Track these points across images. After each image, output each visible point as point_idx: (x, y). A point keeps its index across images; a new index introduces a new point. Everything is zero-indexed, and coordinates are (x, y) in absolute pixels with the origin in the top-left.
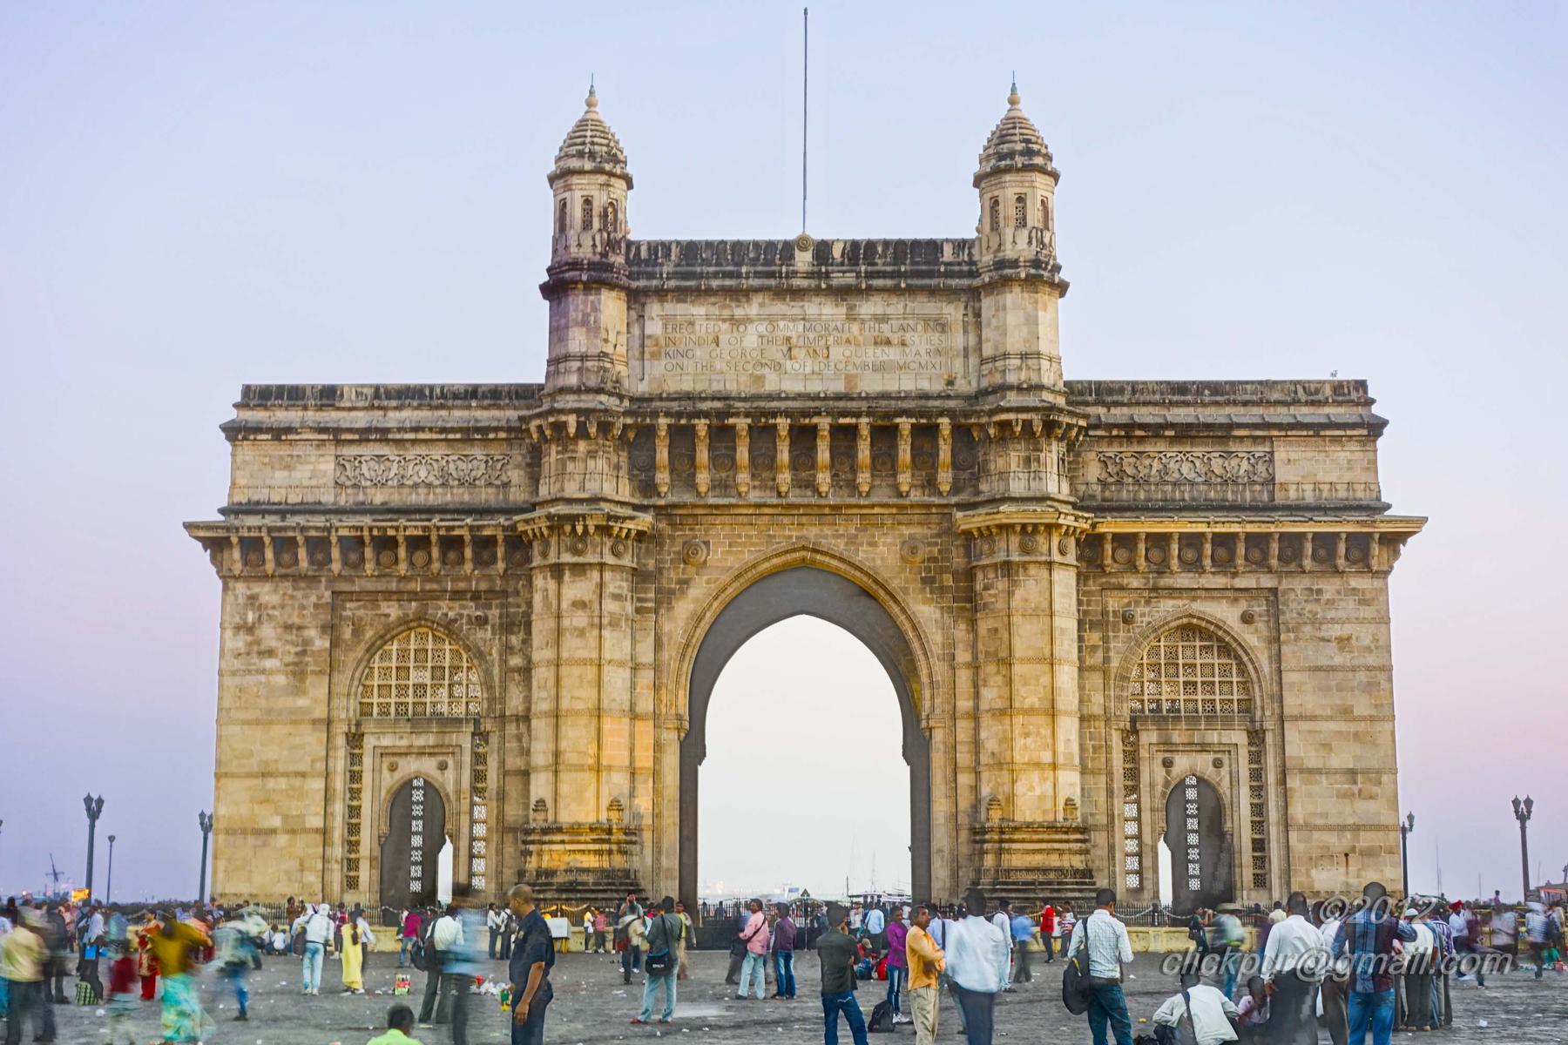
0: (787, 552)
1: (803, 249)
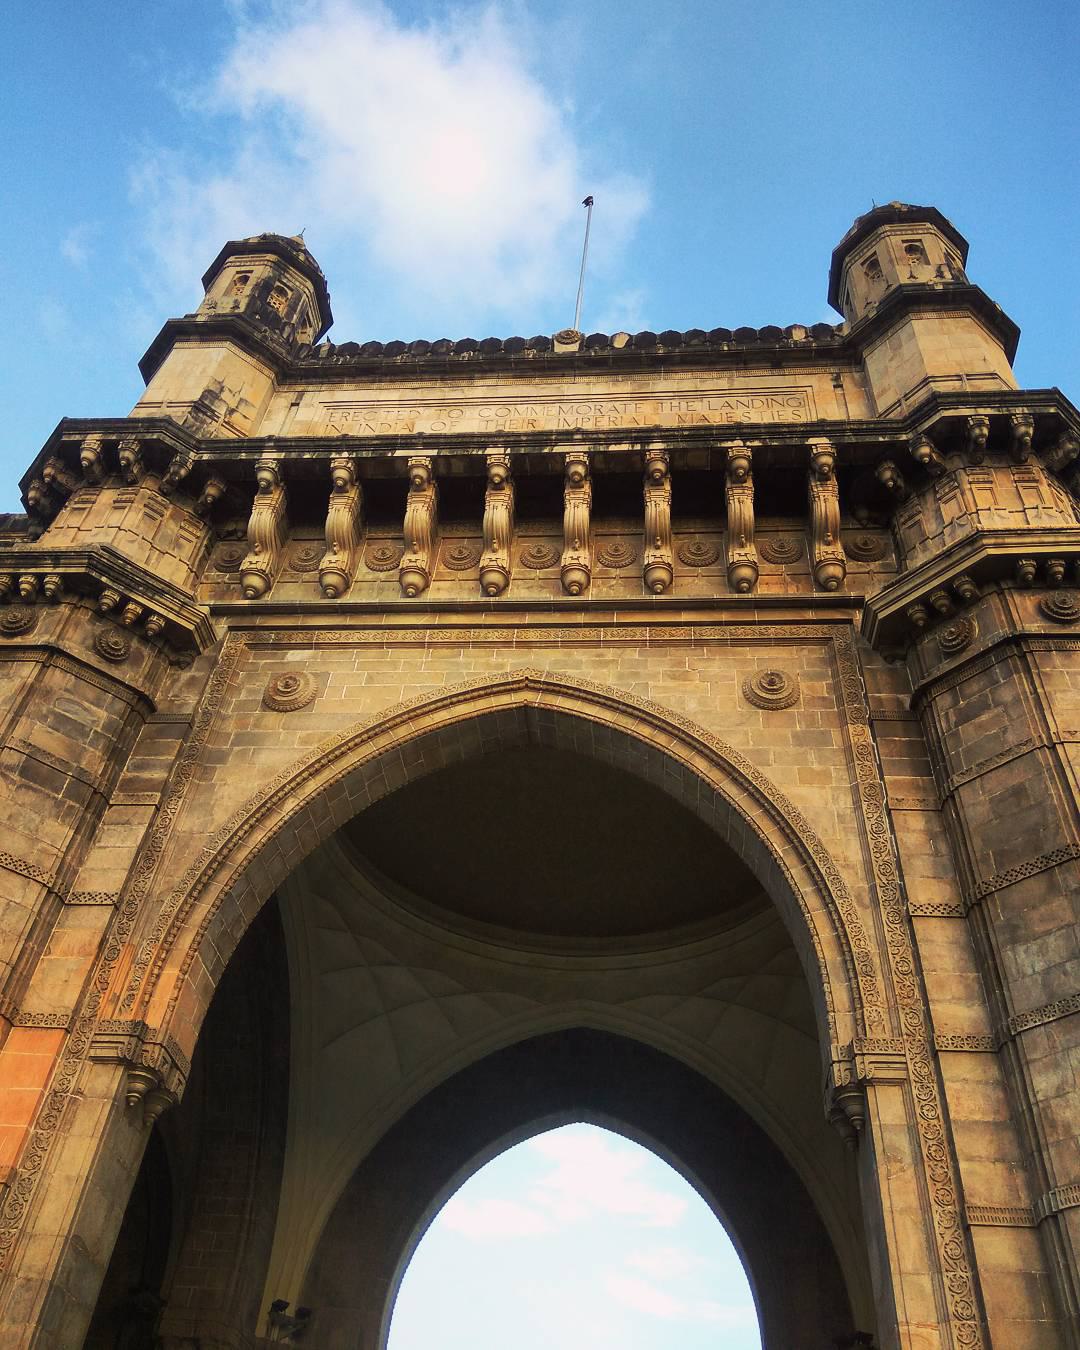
0: (489, 691)
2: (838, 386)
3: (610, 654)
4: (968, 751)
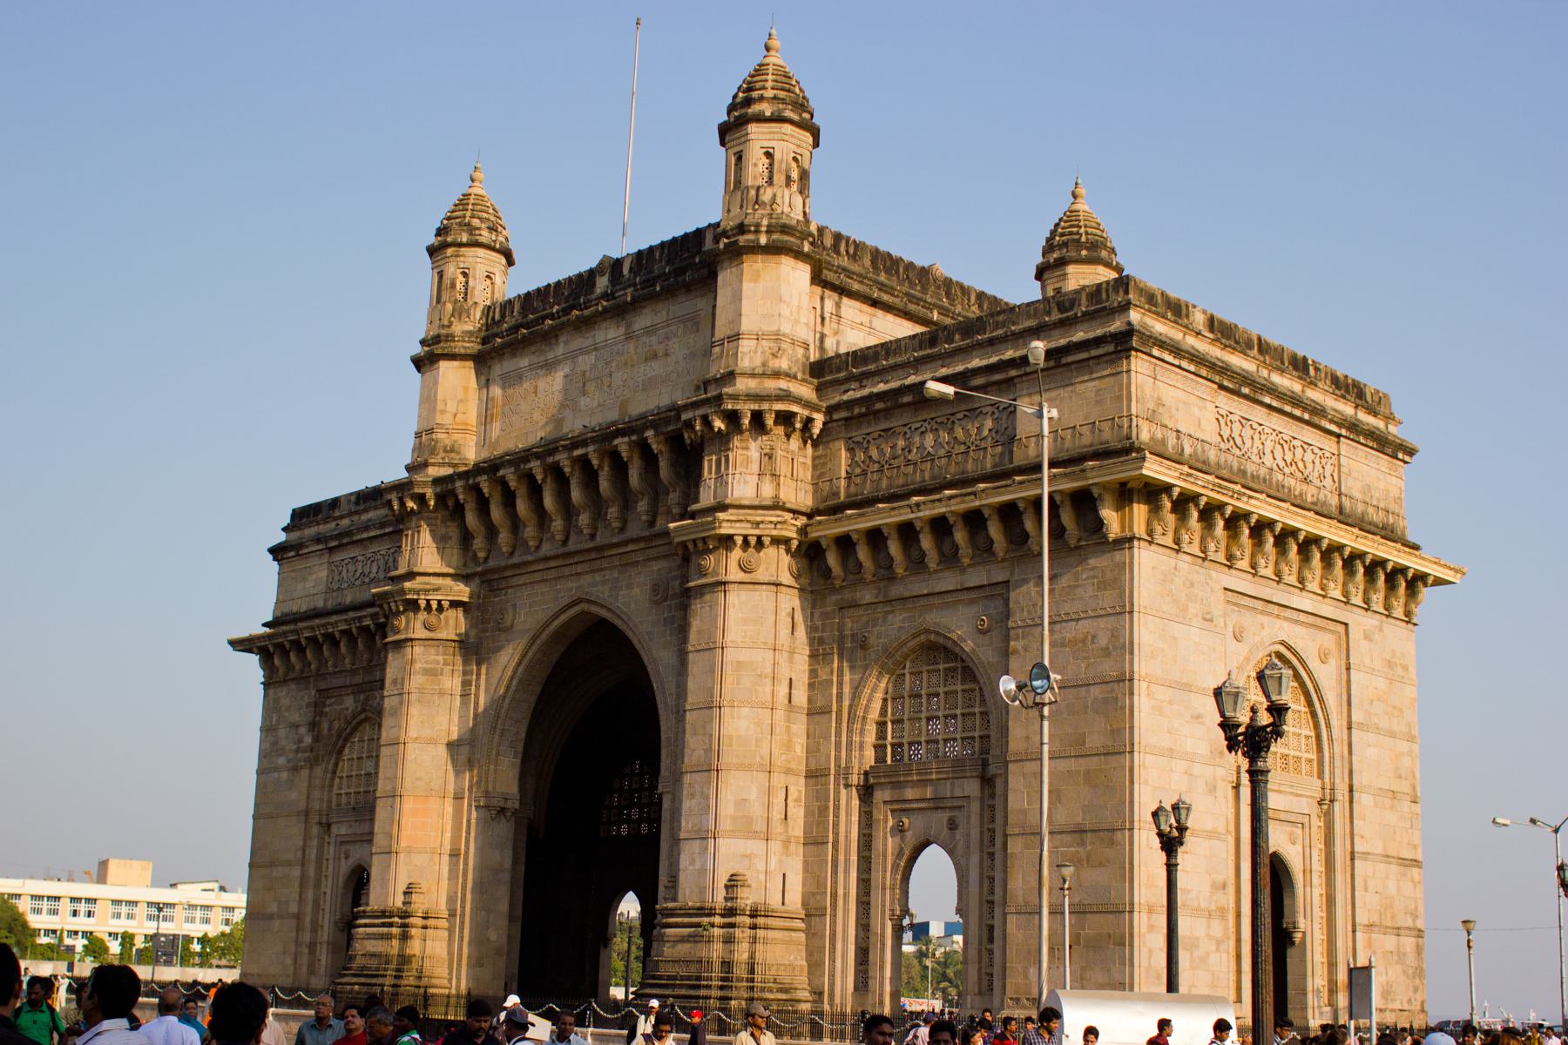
3: (607, 574)
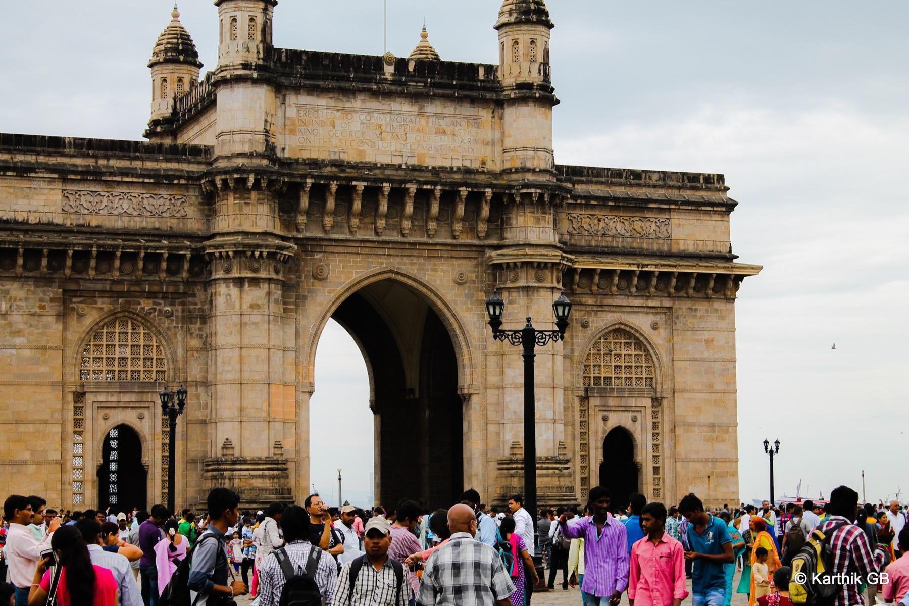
1: (389, 64)
2: (493, 117)
3: (415, 260)
4: (509, 313)
